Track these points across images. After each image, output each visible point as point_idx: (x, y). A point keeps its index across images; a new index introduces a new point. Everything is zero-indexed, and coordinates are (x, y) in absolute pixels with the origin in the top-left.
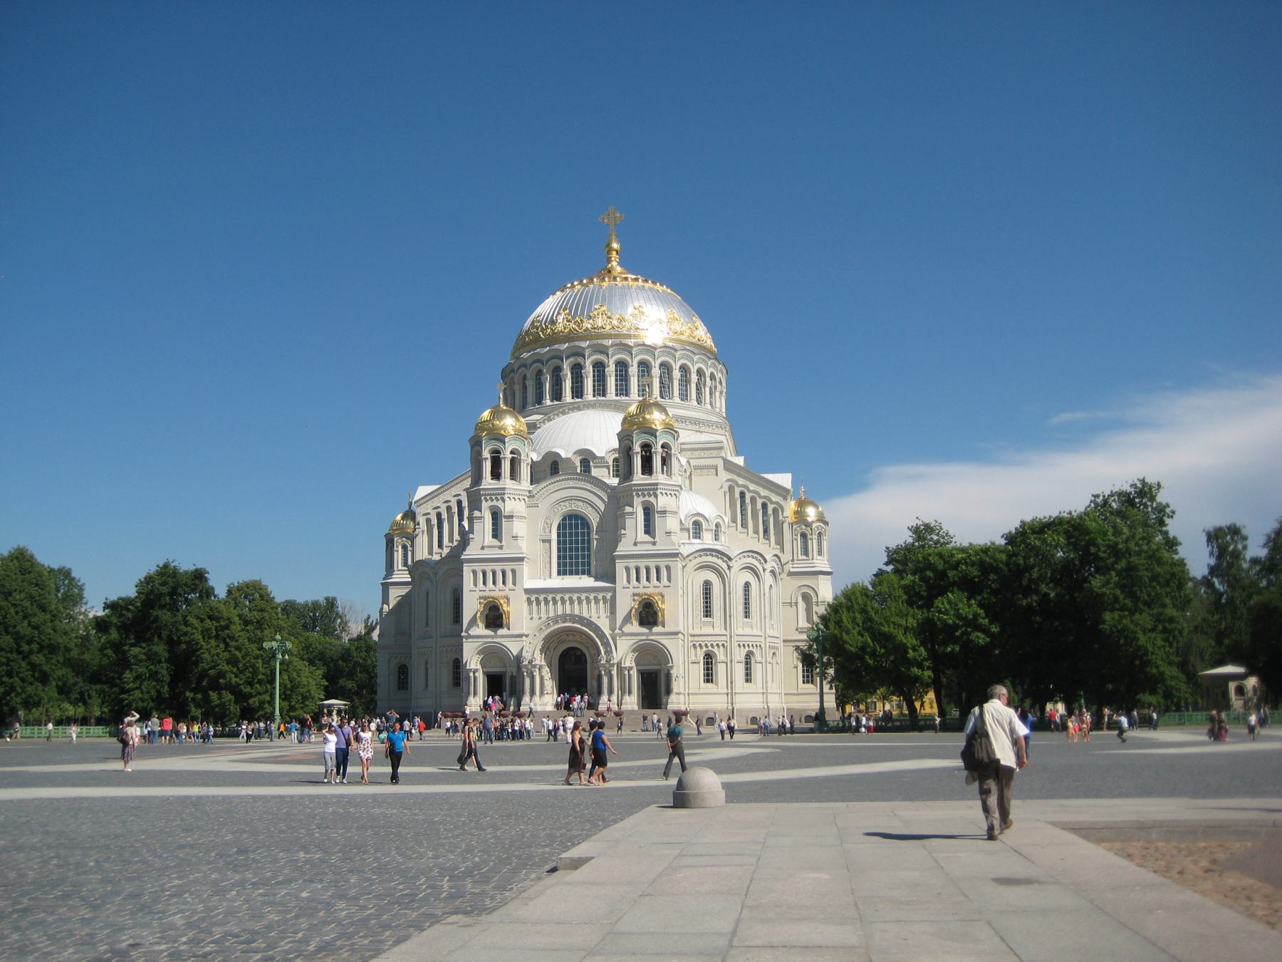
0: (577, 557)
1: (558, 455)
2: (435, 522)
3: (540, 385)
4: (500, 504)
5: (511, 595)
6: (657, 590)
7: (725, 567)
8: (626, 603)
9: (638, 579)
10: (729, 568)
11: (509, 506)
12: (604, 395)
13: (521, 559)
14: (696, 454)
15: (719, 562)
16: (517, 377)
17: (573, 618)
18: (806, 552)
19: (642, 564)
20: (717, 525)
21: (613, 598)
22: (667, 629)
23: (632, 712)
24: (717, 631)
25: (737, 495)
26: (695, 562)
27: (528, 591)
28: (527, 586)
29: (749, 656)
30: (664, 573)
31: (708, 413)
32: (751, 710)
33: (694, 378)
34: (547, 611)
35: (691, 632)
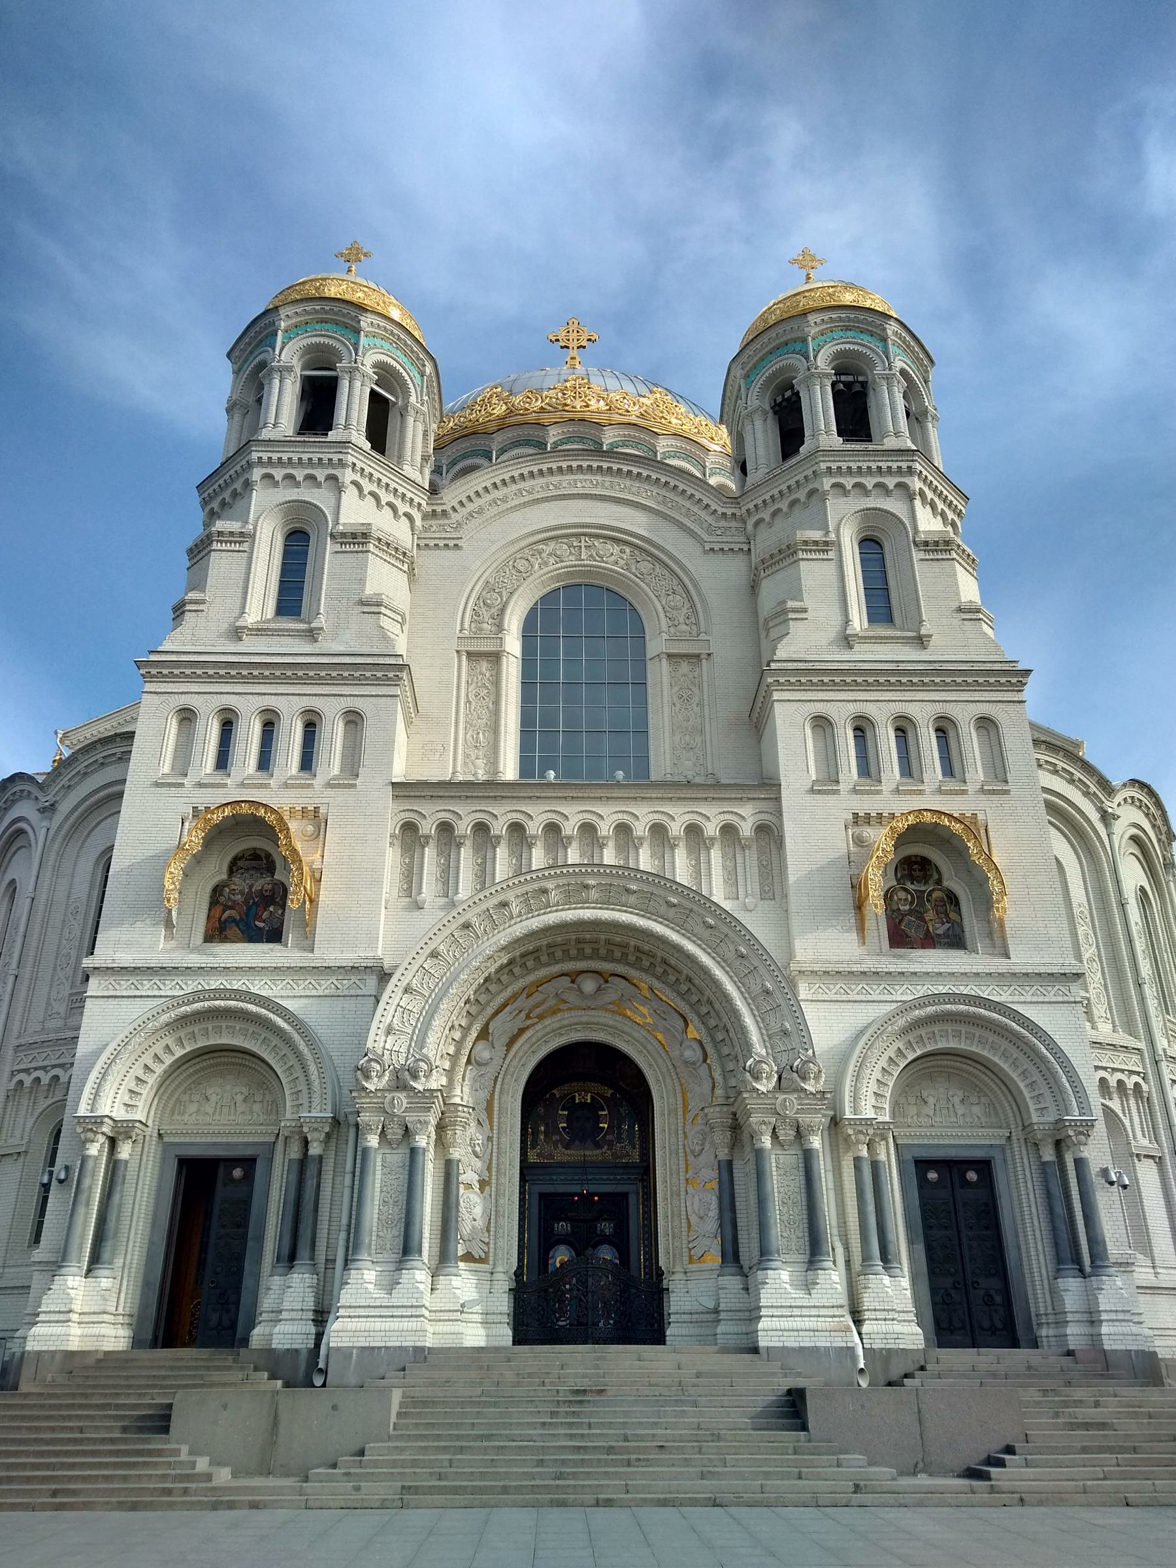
4: (320, 498)
5: (334, 803)
6: (954, 806)
7: (1094, 816)
9: (867, 767)
10: (1107, 818)
11: (354, 511)
13: (386, 672)
17: (620, 884)
19: (882, 710)
21: (770, 834)
22: (1022, 958)
27: (402, 790)
28: (399, 771)
30: (971, 744)
34: (483, 875)
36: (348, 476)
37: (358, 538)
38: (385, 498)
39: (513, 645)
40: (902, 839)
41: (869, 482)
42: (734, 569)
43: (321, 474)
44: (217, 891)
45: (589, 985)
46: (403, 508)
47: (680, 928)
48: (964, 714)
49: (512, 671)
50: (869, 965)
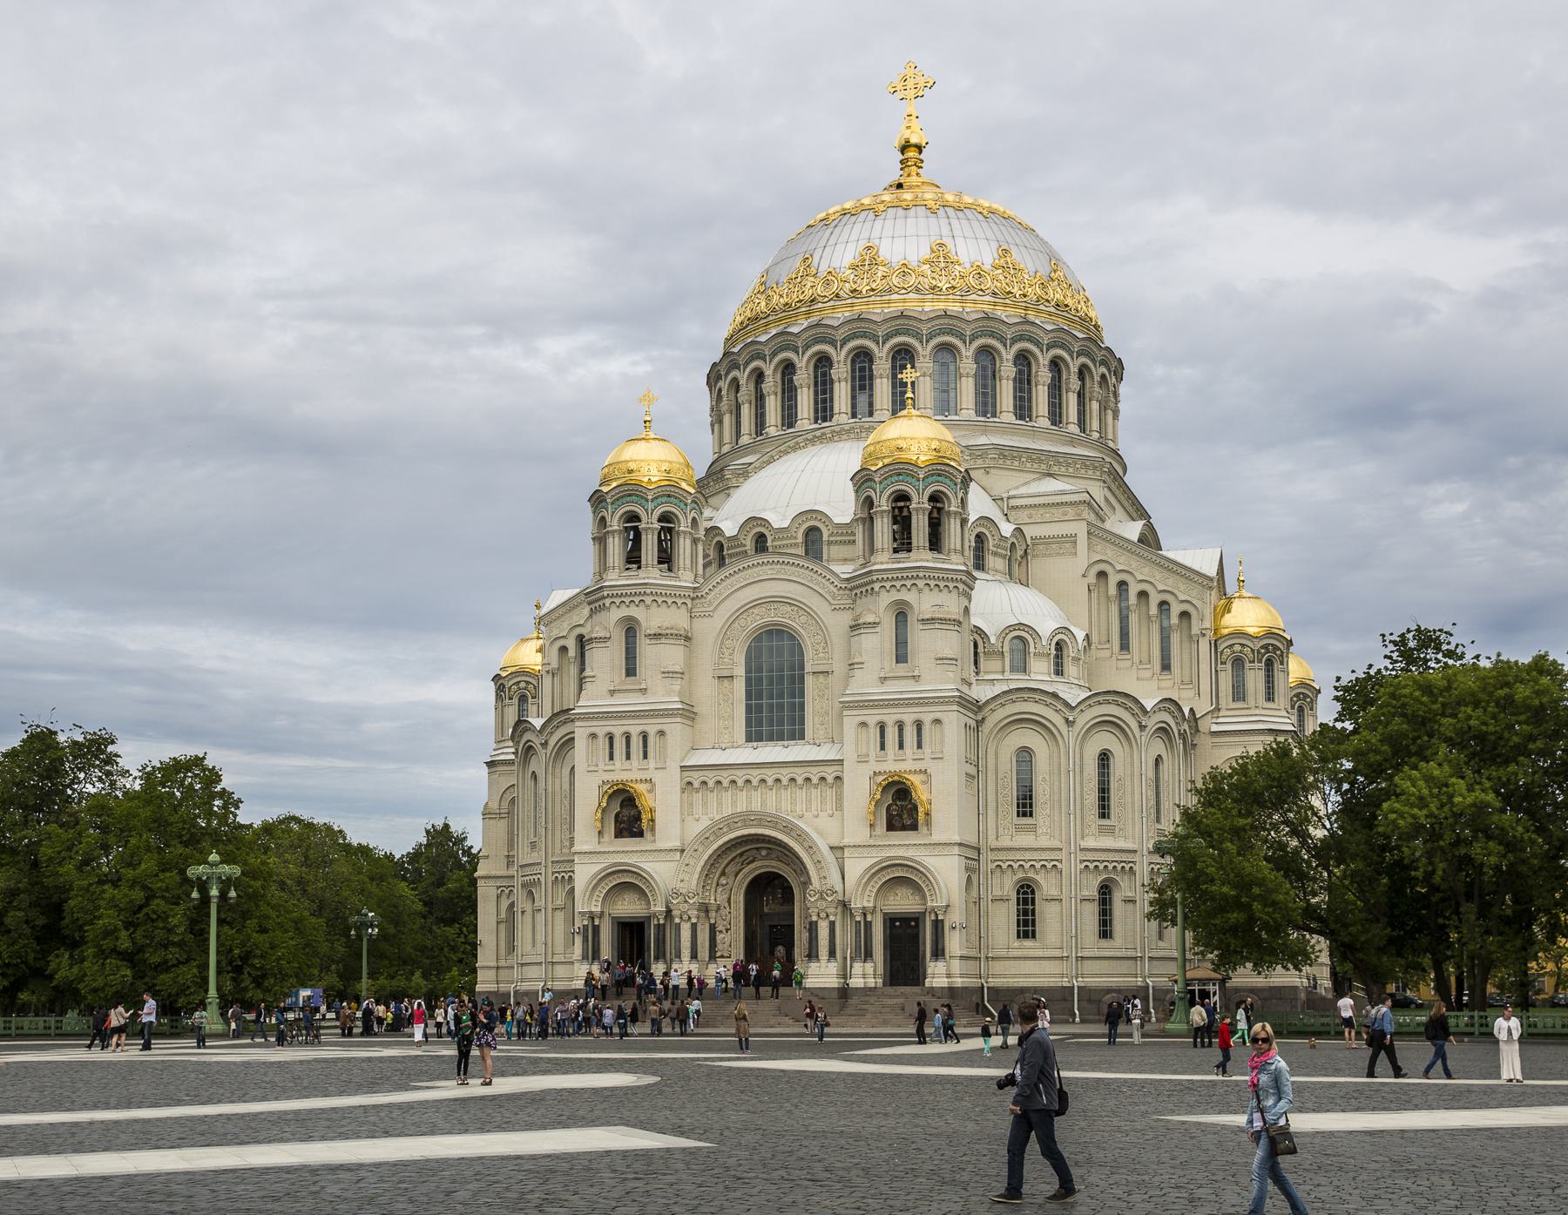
0: (781, 707)
1: (764, 522)
2: (572, 653)
3: (760, 399)
5: (657, 777)
8: (860, 791)
11: (652, 618)
12: (871, 414)
14: (1038, 515)
15: (1048, 713)
16: (723, 385)
17: (761, 819)
18: (1239, 694)
20: (1059, 646)
22: (937, 836)
23: (867, 991)
24: (1044, 842)
25: (1113, 590)
26: (1001, 713)
29: (1106, 891)
31: (1072, 441)
32: (1109, 991)
33: (1043, 375)
35: (993, 843)
36: (648, 600)
37: (657, 636)
38: (670, 601)
39: (740, 671)
40: (885, 789)
41: (898, 584)
42: (846, 619)
43: (637, 599)
44: (617, 816)
45: (764, 853)
46: (679, 601)
47: (788, 834)
48: (927, 719)
49: (740, 687)
50: (871, 842)
